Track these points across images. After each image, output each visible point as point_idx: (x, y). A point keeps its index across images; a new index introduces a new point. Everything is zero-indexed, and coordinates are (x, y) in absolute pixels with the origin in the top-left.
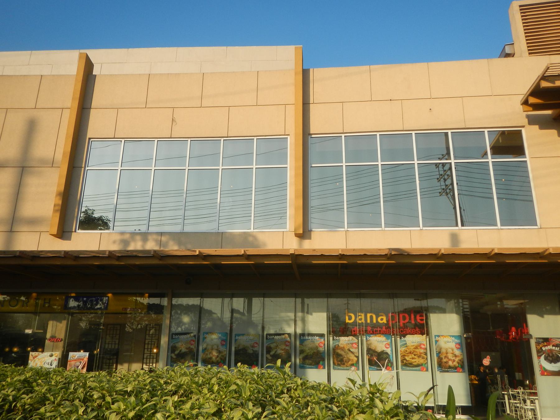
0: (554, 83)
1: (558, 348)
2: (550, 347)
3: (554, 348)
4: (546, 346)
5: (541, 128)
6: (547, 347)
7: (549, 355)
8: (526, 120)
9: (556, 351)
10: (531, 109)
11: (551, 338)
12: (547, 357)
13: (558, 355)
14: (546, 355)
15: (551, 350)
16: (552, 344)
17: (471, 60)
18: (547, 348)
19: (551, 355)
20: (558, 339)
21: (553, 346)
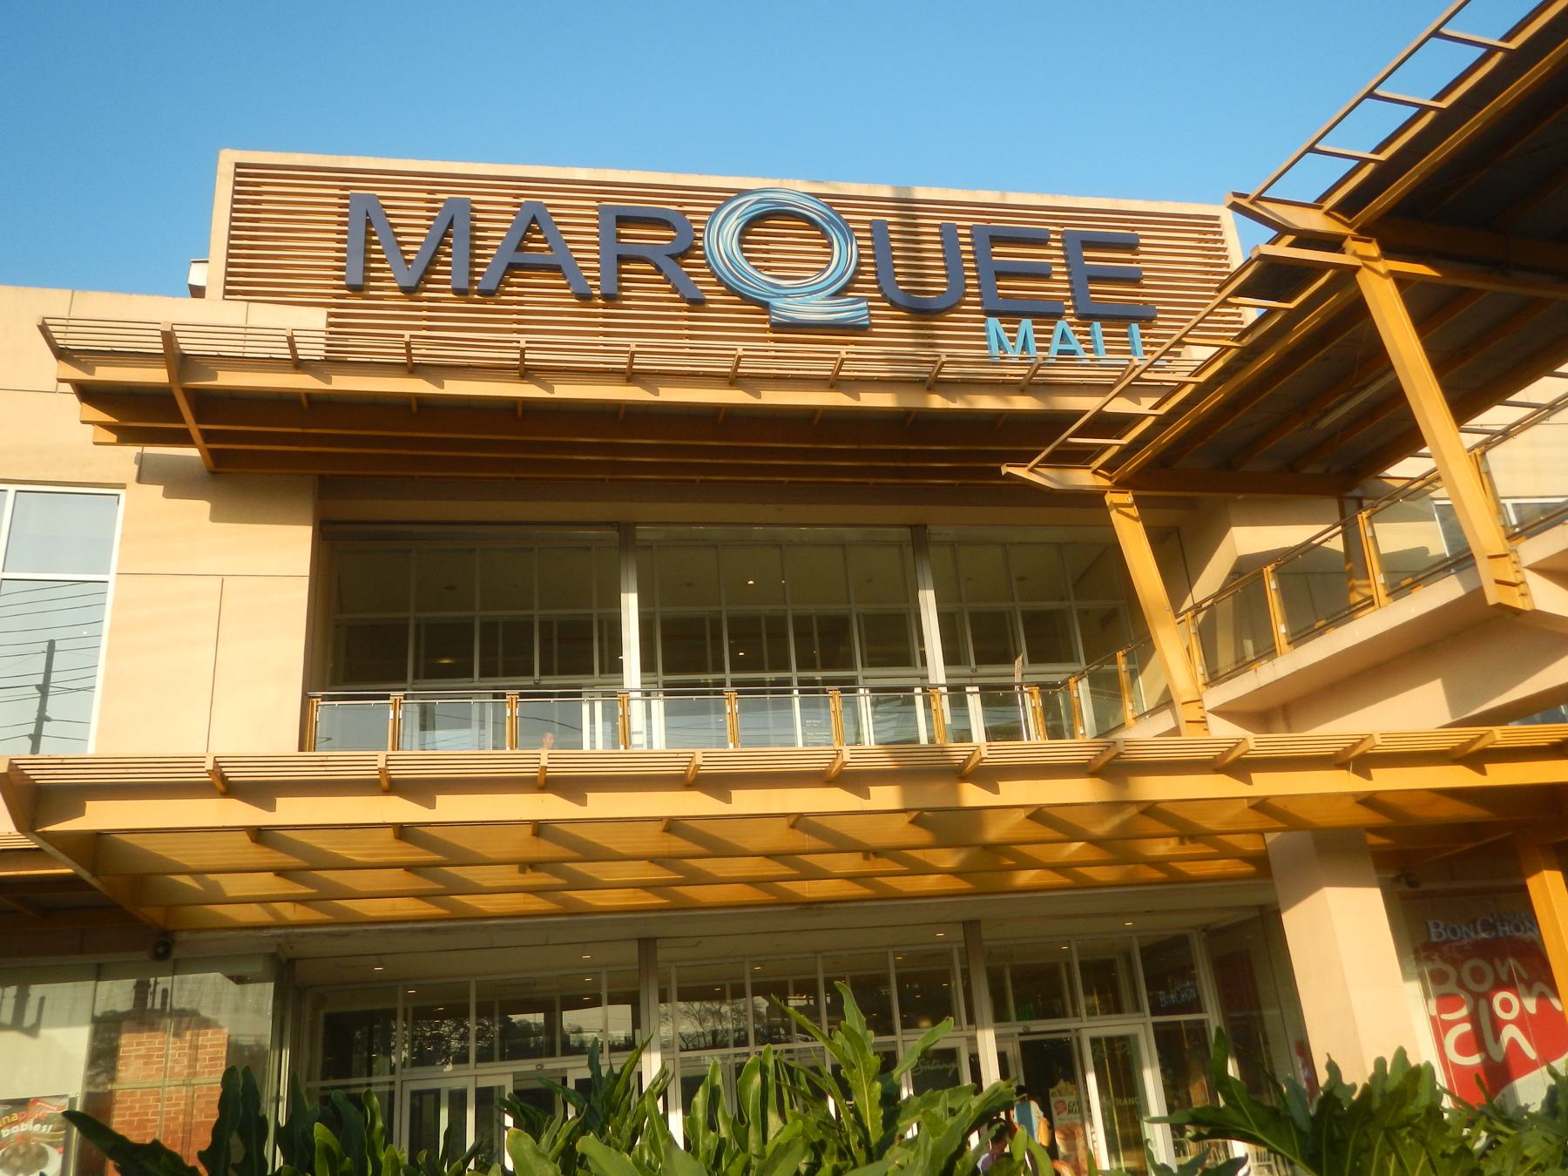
0: (91, 371)
1: (51, 1126)
2: (24, 1127)
3: (38, 1126)
4: (17, 1123)
5: (167, 495)
6: (17, 1127)
7: (15, 1150)
8: (135, 468)
9: (40, 1135)
10: (113, 438)
11: (37, 1099)
12: (10, 1157)
13: (45, 1148)
14: (8, 1153)
15: (25, 1138)
16: (36, 1116)
17: (22, 288)
18: (16, 1130)
19: (22, 1150)
20: (58, 1099)
21: (36, 1122)
